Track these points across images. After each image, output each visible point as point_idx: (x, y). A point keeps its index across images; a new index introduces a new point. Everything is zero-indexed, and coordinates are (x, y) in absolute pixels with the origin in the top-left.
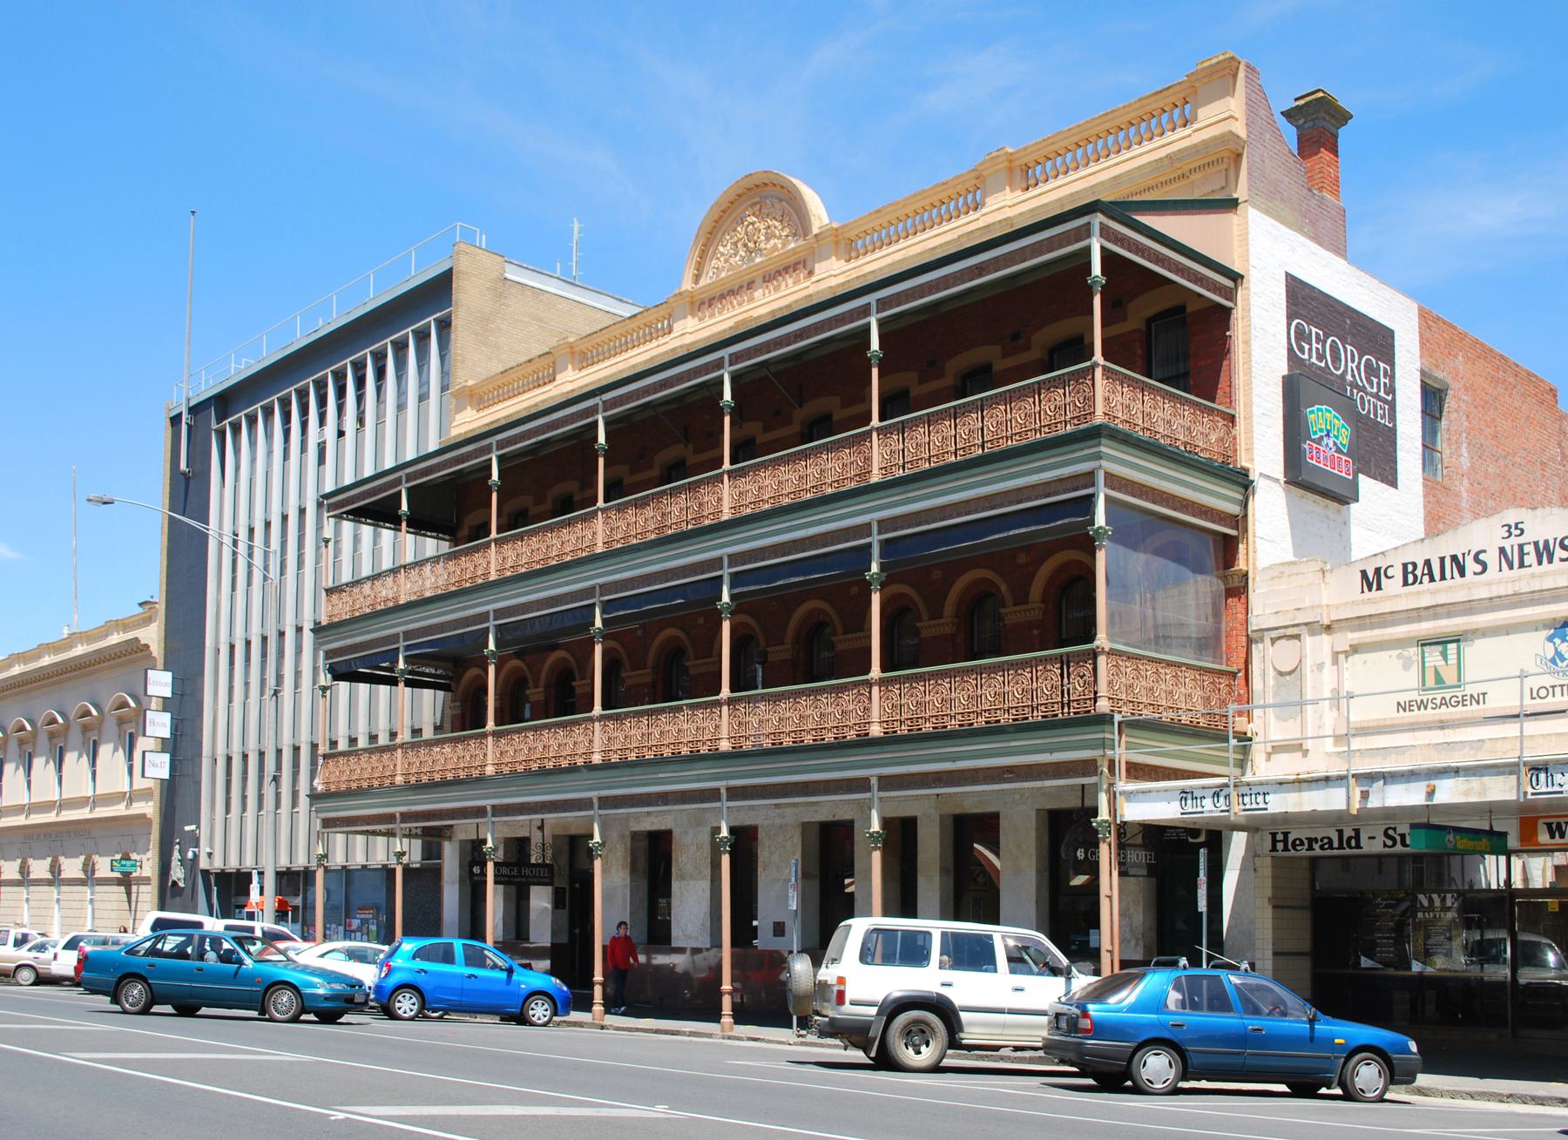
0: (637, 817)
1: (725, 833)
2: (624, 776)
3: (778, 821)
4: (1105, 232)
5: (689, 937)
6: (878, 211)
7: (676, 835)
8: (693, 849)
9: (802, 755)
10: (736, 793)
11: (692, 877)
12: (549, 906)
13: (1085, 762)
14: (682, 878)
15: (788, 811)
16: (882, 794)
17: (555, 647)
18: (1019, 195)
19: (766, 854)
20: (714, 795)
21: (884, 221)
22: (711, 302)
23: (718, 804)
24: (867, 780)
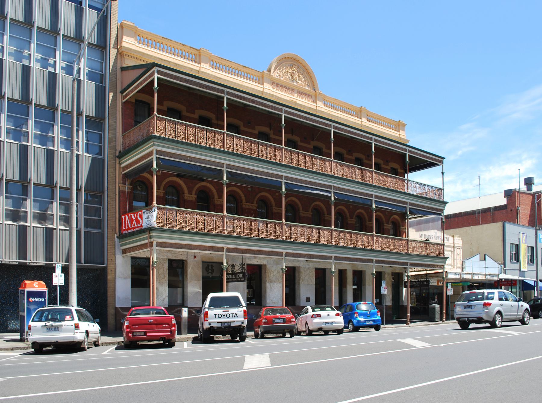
0: (250, 259)
1: (284, 268)
2: (347, 251)
3: (307, 266)
4: (159, 72)
5: (275, 303)
6: (184, 45)
7: (268, 266)
8: (275, 272)
9: (296, 245)
10: (378, 262)
11: (275, 282)
12: (201, 291)
13: (280, 252)
14: (271, 282)
15: (311, 264)
16: (286, 258)
17: (203, 180)
18: (136, 43)
19: (303, 276)
20: (371, 261)
21: (335, 102)
22: (277, 85)
23: (222, 253)
24: (223, 248)
